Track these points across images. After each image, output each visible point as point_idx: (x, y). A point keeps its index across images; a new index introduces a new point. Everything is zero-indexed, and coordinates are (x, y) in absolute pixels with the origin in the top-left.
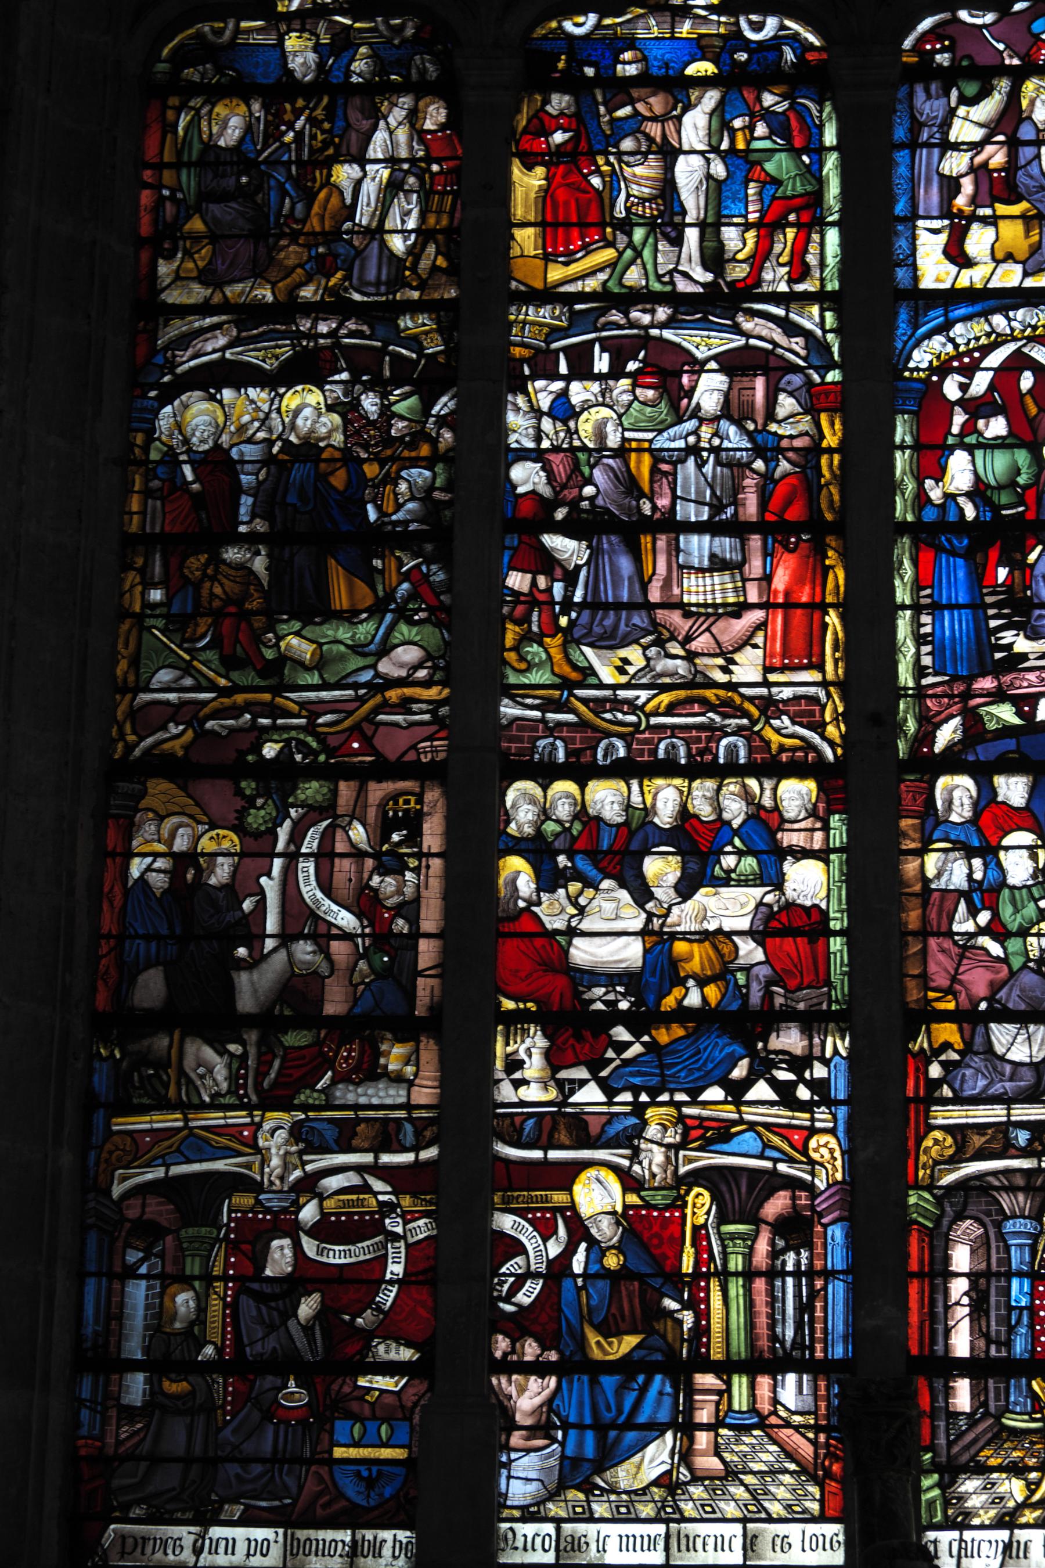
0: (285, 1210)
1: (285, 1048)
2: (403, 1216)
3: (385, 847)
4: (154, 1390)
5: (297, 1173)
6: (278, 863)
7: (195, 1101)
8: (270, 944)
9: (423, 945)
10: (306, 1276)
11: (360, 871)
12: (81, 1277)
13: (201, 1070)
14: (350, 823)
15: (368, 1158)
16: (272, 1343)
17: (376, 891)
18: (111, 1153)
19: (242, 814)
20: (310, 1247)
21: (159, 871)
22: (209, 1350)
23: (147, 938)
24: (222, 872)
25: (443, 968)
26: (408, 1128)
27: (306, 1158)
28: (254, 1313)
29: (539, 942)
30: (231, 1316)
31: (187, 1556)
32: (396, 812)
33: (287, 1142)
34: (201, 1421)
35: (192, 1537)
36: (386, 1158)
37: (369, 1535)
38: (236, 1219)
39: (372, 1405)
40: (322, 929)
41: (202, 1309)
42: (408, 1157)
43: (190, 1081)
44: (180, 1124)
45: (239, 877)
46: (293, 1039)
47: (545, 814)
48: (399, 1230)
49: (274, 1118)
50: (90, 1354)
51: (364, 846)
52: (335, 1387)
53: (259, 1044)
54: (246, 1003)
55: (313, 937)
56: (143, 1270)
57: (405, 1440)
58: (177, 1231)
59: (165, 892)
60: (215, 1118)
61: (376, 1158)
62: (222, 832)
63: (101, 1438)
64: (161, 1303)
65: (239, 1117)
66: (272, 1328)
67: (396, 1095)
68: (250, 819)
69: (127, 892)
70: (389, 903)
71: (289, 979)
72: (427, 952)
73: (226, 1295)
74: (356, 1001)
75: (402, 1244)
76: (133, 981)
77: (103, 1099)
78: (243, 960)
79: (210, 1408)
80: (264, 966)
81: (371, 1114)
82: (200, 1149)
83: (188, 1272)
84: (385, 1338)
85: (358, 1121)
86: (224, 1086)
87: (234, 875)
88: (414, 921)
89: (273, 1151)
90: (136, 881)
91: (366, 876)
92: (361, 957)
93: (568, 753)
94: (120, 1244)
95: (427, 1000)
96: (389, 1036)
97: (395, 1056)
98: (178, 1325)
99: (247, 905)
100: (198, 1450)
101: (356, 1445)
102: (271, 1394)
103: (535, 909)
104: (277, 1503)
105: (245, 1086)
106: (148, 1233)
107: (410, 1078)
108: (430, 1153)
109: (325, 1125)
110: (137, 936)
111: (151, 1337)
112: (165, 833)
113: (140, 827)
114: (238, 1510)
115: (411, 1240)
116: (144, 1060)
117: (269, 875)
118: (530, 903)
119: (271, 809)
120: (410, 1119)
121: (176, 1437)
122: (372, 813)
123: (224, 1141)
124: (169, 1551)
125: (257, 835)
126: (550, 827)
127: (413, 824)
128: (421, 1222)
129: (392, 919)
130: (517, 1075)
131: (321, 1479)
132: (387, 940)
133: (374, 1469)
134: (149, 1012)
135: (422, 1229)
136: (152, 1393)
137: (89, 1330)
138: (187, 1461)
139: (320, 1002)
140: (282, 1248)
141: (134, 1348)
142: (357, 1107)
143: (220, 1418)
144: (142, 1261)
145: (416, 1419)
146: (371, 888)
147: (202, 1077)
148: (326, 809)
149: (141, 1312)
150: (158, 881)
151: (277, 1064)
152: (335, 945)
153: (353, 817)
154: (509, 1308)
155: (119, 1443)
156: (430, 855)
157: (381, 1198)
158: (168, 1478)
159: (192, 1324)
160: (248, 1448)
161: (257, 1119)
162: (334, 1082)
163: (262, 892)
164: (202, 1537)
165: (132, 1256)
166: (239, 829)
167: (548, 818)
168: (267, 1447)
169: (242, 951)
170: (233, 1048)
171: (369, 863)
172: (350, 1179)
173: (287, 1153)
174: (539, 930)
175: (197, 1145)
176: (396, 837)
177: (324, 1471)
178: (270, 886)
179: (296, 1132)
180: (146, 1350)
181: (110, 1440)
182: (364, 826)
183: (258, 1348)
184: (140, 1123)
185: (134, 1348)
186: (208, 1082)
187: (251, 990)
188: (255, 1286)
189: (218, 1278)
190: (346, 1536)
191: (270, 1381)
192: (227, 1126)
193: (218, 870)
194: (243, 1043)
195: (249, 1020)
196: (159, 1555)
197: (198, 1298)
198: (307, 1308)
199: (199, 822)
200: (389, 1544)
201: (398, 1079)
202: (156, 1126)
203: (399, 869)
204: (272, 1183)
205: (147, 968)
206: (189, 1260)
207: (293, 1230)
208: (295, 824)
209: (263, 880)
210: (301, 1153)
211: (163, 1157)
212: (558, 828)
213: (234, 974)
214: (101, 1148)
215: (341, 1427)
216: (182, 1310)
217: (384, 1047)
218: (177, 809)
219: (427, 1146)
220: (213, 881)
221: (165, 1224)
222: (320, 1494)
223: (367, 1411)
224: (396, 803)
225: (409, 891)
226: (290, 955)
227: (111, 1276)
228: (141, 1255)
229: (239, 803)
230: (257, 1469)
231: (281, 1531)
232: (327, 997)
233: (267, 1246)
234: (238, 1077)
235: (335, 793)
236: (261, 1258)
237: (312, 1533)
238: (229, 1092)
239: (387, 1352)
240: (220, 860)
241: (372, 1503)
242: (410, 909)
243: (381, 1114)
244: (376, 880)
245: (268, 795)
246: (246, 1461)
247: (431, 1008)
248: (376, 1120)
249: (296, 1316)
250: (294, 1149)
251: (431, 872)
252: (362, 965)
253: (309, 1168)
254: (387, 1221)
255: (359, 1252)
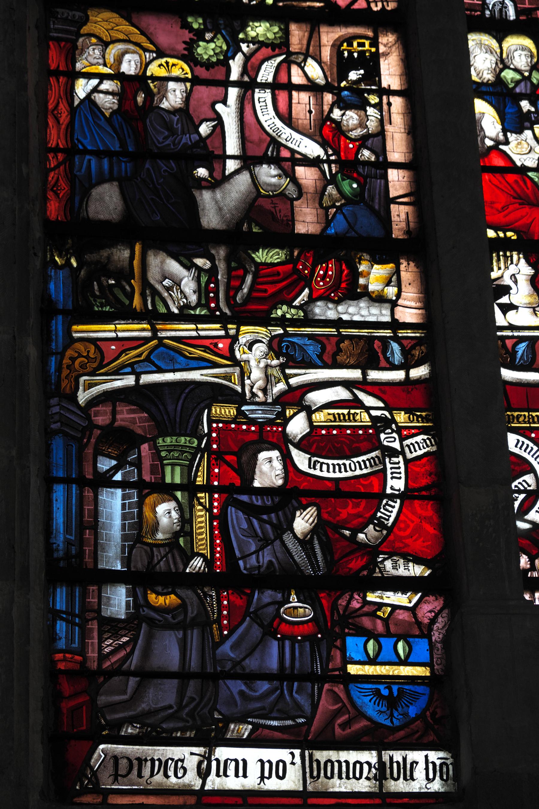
0: (271, 422)
1: (258, 265)
2: (399, 430)
3: (344, 84)
4: (138, 604)
5: (281, 386)
6: (233, 93)
7: (162, 310)
8: (231, 166)
9: (393, 174)
10: (297, 490)
11: (320, 103)
12: (49, 482)
13: (167, 282)
14: (305, 60)
15: (355, 374)
16: (266, 556)
17: (338, 124)
18: (73, 359)
19: (191, 45)
20: (301, 460)
21: (107, 93)
22: (197, 563)
23: (98, 154)
24: (174, 96)
25: (417, 196)
26: (395, 346)
27: (288, 371)
28: (245, 526)
29: (511, 178)
30: (220, 528)
31: (192, 779)
32: (350, 53)
33: (266, 356)
34: (195, 635)
35: (196, 759)
36: (374, 375)
37: (398, 756)
38: (217, 430)
39: (386, 621)
40: (285, 154)
41: (186, 520)
42: (399, 375)
43: (155, 293)
44: (148, 334)
45: (192, 102)
46: (262, 256)
47: (503, 63)
48: (396, 445)
49: (247, 332)
50: (62, 564)
51: (321, 81)
52: (342, 602)
53: (228, 260)
54: (211, 219)
55: (276, 161)
56: (118, 477)
57: (425, 657)
58: (154, 440)
59: (114, 113)
60: (186, 330)
61: (364, 374)
62: (171, 61)
63: (82, 651)
64: (140, 513)
65: (213, 330)
66: (265, 542)
67: (380, 314)
68: (200, 50)
69: (73, 111)
70: (354, 134)
71: (255, 200)
72: (397, 181)
73: (211, 506)
74: (328, 223)
75: (401, 459)
76: (86, 194)
77: (61, 307)
78: (204, 179)
79: (203, 623)
80: (227, 186)
81: (354, 332)
82: (172, 360)
83: (168, 480)
84: (390, 555)
85: (342, 338)
86: (193, 299)
87: (187, 99)
88: (381, 151)
89: (253, 363)
90: (82, 101)
91: (326, 108)
92: (329, 183)
93: (518, 12)
94: (89, 451)
95: (403, 225)
96: (366, 256)
97: (375, 276)
98: (160, 536)
99: (204, 129)
100: (194, 664)
101: (372, 662)
102: (271, 609)
103: (501, 147)
104: (289, 722)
105: (216, 299)
106: (122, 442)
107: (392, 296)
108: (419, 372)
109: (307, 341)
110: (85, 152)
111: (131, 548)
112: (110, 57)
113: (82, 52)
114: (246, 730)
115: (409, 456)
116: (104, 269)
117: (224, 102)
118: (498, 142)
119: (220, 43)
120: (396, 339)
121: (168, 651)
122: (326, 53)
123: (199, 352)
124: (171, 773)
125: (208, 65)
126: (509, 75)
127: (371, 65)
128: (419, 438)
129: (358, 151)
130: (504, 300)
131: (336, 699)
132: (355, 165)
133: (395, 688)
134: (106, 223)
135: (420, 445)
136: (137, 605)
137: (60, 539)
138: (183, 676)
139: (292, 221)
140: (270, 460)
141: (113, 560)
142: (339, 323)
143: (216, 632)
144: (115, 469)
145: (436, 636)
146: (333, 121)
147: (168, 289)
148: (281, 45)
149: (117, 522)
150: (107, 102)
151: (249, 279)
152: (301, 171)
153: (307, 55)
154: (521, 525)
155: (103, 658)
156: (389, 92)
157: (374, 413)
158: (163, 695)
159: (176, 535)
160: (252, 664)
161: (232, 332)
162: (312, 299)
163: (218, 118)
164: (208, 757)
165: (105, 464)
166: (189, 57)
167: (506, 67)
168: (273, 664)
169: (202, 172)
170: (199, 262)
171: (328, 98)
172: (340, 393)
173: (267, 366)
174: (510, 165)
175: (168, 355)
176: (353, 75)
177: (339, 689)
178: (228, 113)
179: (275, 347)
180: (127, 561)
181: (93, 654)
182: (320, 62)
183: (253, 561)
184: (105, 331)
185: (113, 560)
186: (175, 294)
187: (214, 208)
188: (244, 498)
189: (202, 488)
190: (371, 757)
191: (268, 596)
192: (199, 337)
193: (170, 96)
194: (212, 259)
195: (216, 237)
196: (159, 778)
197: (180, 508)
198: (302, 523)
199: (145, 50)
200: (422, 765)
201: (379, 299)
202: (120, 335)
203: (361, 105)
204: (254, 395)
205: (101, 181)
206: (168, 469)
207: (282, 443)
208: (247, 58)
209: (219, 107)
210: (282, 367)
211: (131, 365)
212: (518, 77)
213: (196, 193)
214: (62, 355)
215: (354, 644)
216: (164, 521)
217: (363, 267)
218: (121, 36)
219: (417, 365)
220: (165, 105)
221: (139, 431)
222: (337, 714)
223: (380, 627)
224: (350, 44)
225: (372, 125)
226: (254, 178)
227: (82, 482)
228: (114, 463)
229: (187, 36)
230: (264, 686)
231: (297, 752)
232: (298, 217)
233: (256, 459)
234: (208, 290)
235: (286, 33)
236: (249, 470)
237: (333, 755)
238: (199, 304)
239: (395, 568)
240: (171, 85)
241: (396, 723)
242: (377, 139)
243: (364, 332)
244: (337, 114)
245: (216, 31)
246: (250, 678)
247: (408, 232)
248: (360, 337)
249: (292, 530)
250: (275, 362)
251: (393, 109)
252: (331, 189)
253: (292, 381)
254: (383, 436)
255: (354, 467)
